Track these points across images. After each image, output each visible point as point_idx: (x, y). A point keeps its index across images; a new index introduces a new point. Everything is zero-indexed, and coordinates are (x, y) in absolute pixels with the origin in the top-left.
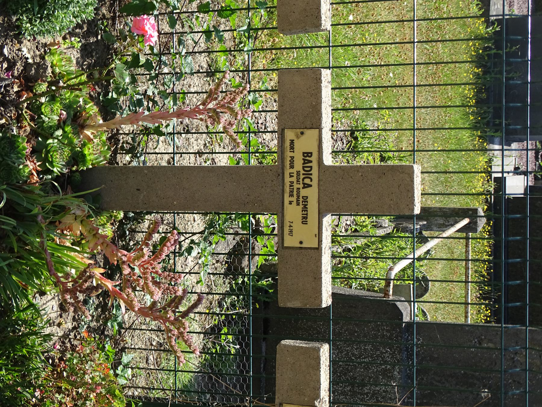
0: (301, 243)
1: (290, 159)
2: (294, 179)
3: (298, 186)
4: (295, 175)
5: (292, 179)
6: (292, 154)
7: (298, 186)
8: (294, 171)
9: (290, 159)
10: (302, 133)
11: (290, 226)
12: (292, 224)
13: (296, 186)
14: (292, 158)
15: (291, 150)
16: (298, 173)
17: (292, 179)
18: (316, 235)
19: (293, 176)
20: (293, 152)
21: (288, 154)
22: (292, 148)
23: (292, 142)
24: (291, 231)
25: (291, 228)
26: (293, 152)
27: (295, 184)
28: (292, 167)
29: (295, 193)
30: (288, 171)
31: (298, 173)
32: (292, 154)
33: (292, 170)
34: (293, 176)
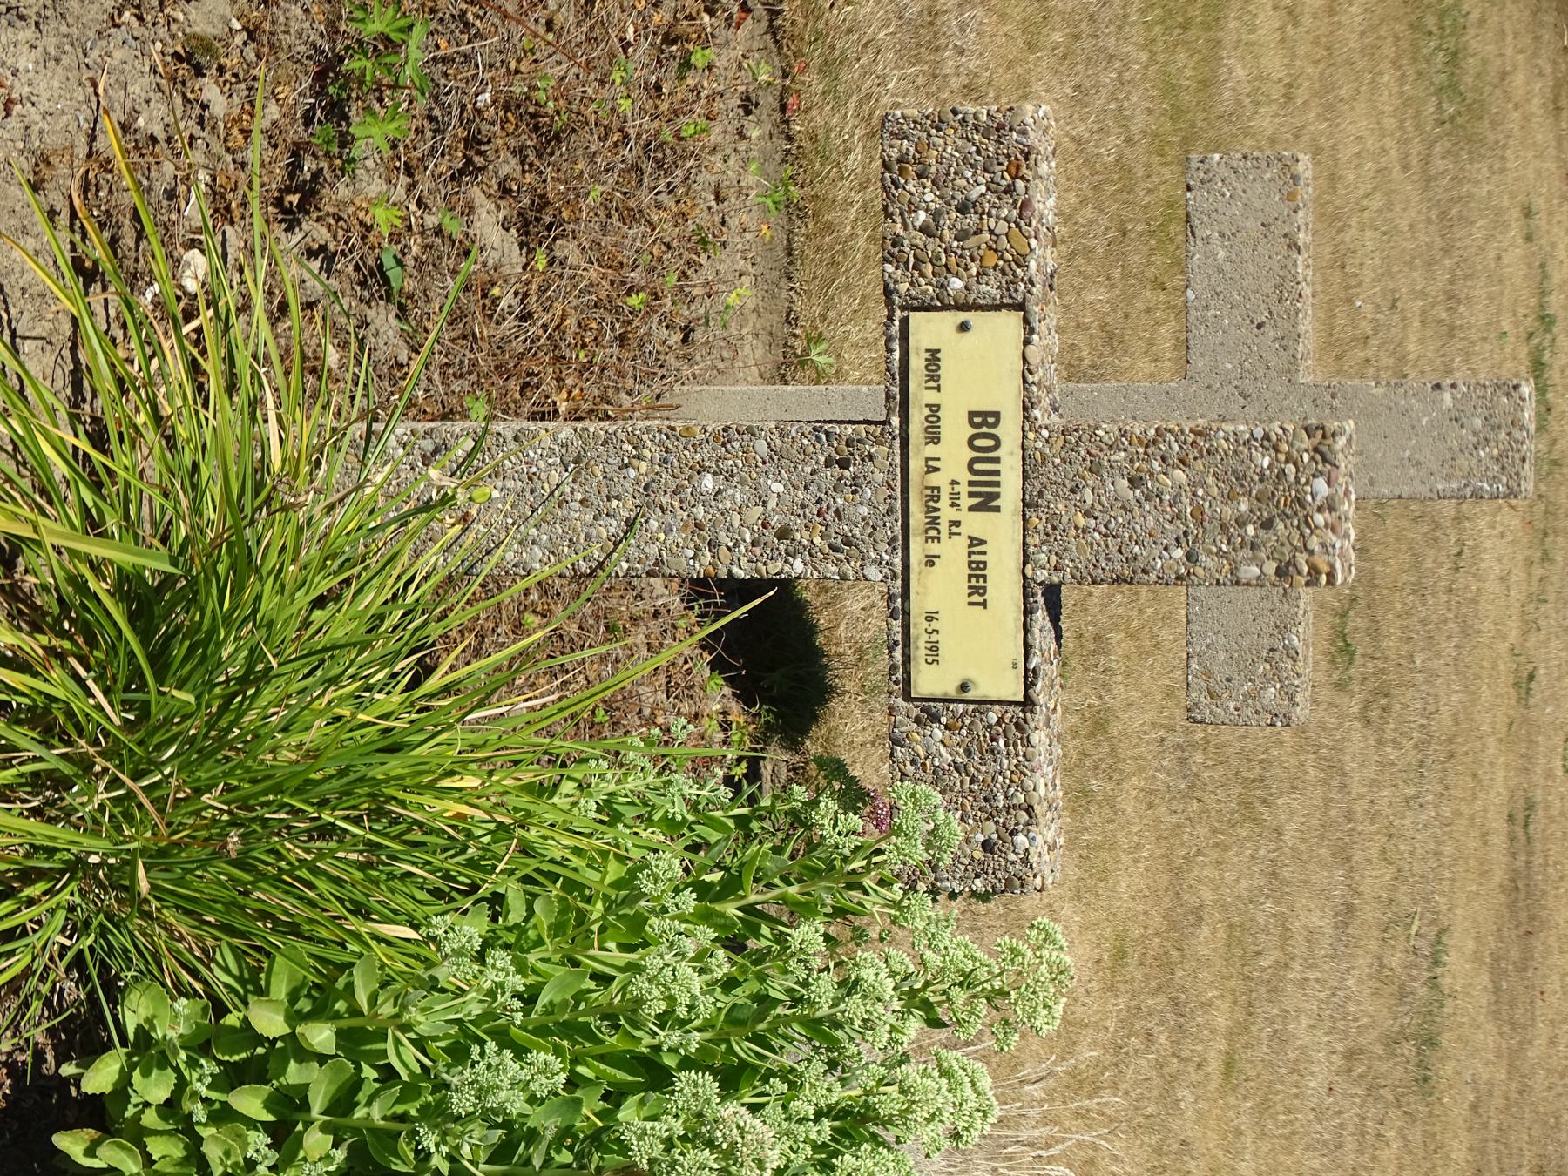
1: (927, 411)
5: (934, 479)
6: (932, 397)
9: (927, 411)
14: (934, 409)
15: (932, 384)
17: (934, 479)
19: (937, 469)
20: (938, 389)
21: (921, 396)
22: (933, 376)
23: (934, 355)
24: (934, 648)
25: (934, 637)
26: (938, 389)
28: (934, 439)
32: (932, 397)
33: (931, 451)
34: (937, 469)
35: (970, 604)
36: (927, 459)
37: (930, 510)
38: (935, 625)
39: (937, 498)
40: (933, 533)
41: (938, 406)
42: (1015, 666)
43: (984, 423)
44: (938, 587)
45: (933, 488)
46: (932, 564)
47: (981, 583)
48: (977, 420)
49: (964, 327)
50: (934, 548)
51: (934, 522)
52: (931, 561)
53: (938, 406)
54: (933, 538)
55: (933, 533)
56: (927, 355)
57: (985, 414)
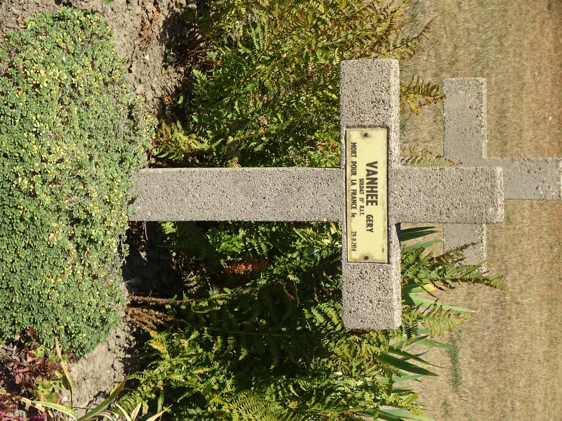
0: (366, 258)
2: (357, 187)
3: (362, 196)
4: (358, 182)
5: (353, 187)
6: (354, 159)
7: (362, 196)
8: (357, 178)
10: (366, 135)
11: (355, 240)
12: (355, 237)
13: (358, 196)
14: (354, 163)
15: (353, 155)
16: (361, 181)
17: (353, 187)
18: (383, 250)
19: (355, 184)
20: (356, 156)
21: (350, 159)
22: (354, 152)
23: (354, 145)
24: (355, 245)
25: (355, 242)
26: (356, 156)
27: (358, 192)
28: (354, 173)
30: (350, 177)
31: (361, 181)
32: (354, 159)
33: (353, 177)
34: (355, 184)
35: (367, 230)
36: (352, 180)
37: (353, 198)
38: (355, 237)
40: (354, 206)
42: (383, 251)
44: (357, 224)
45: (354, 190)
46: (353, 216)
47: (371, 222)
50: (354, 211)
51: (354, 202)
52: (353, 216)
54: (354, 208)
55: (354, 206)
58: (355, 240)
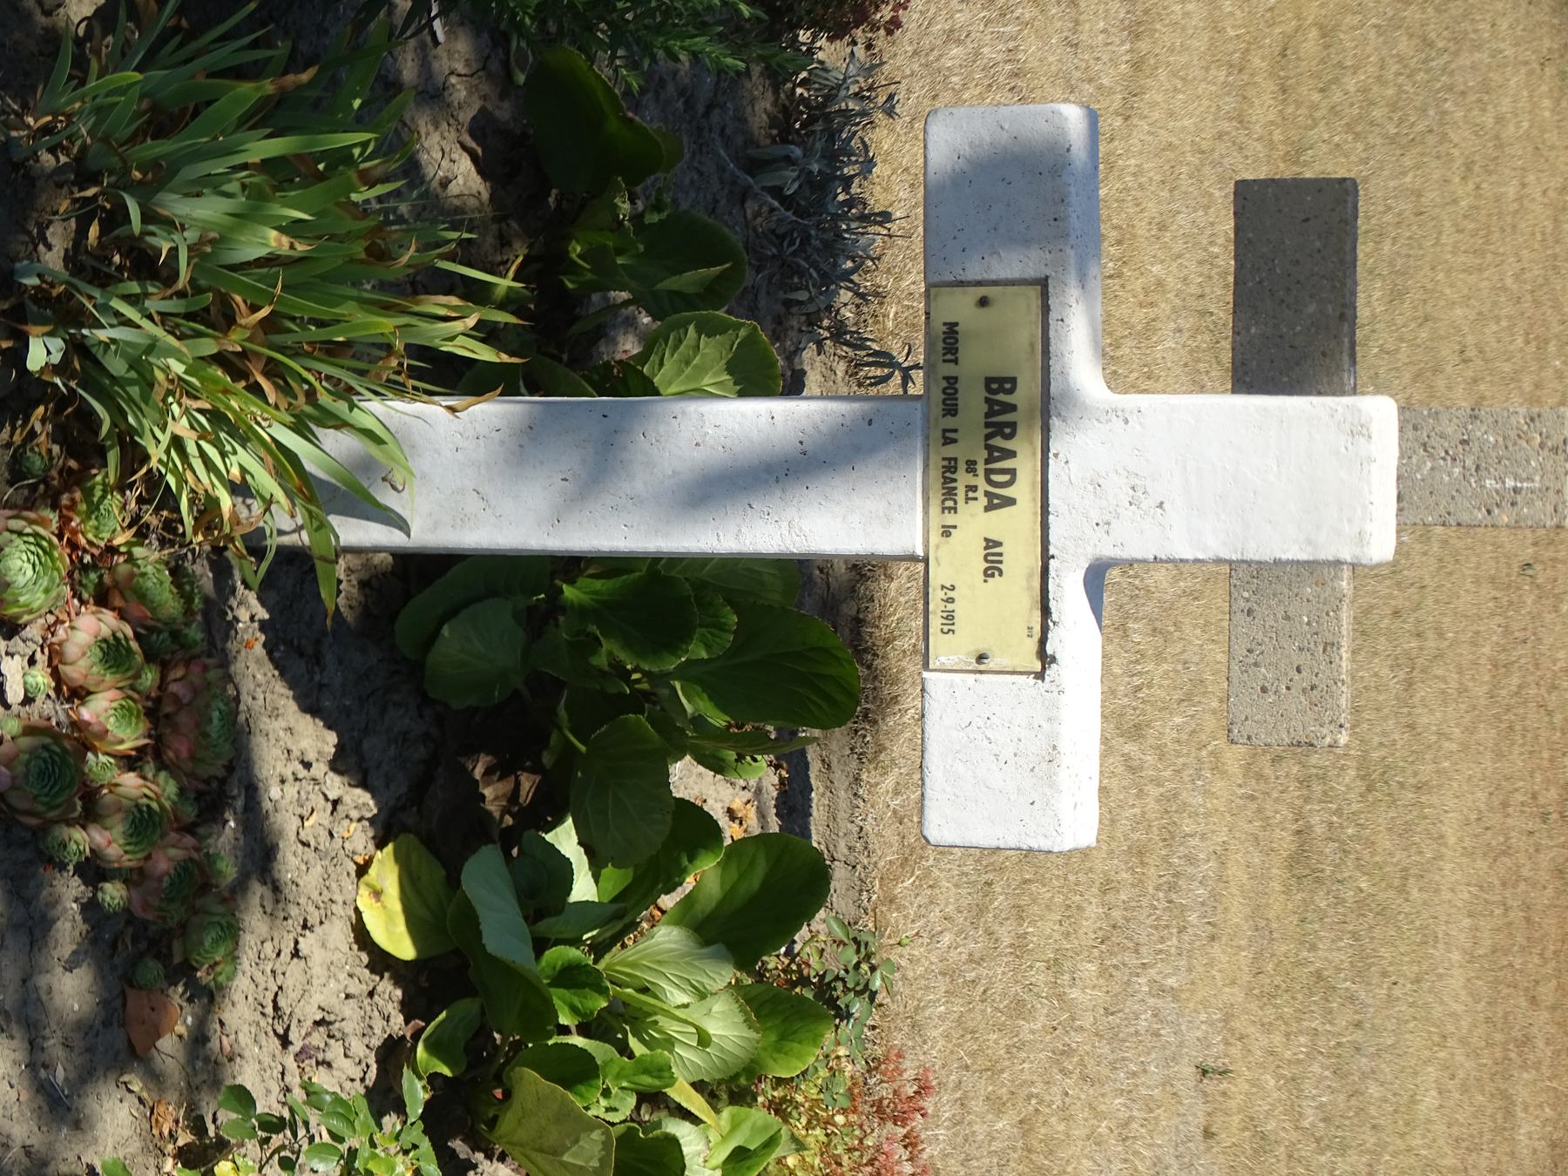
1: (944, 384)
5: (950, 451)
9: (944, 384)
11: (951, 600)
12: (950, 594)
14: (952, 381)
15: (949, 357)
20: (956, 361)
24: (949, 617)
25: (950, 607)
26: (956, 361)
28: (951, 409)
29: (961, 496)
32: (950, 370)
34: (954, 441)
36: (945, 431)
37: (947, 480)
38: (950, 594)
39: (954, 469)
40: (950, 504)
41: (956, 378)
43: (1002, 390)
45: (950, 460)
48: (994, 386)
49: (983, 302)
50: (950, 519)
52: (947, 532)
53: (956, 378)
54: (950, 509)
55: (950, 504)
56: (944, 329)
57: (1001, 381)
58: (951, 600)
